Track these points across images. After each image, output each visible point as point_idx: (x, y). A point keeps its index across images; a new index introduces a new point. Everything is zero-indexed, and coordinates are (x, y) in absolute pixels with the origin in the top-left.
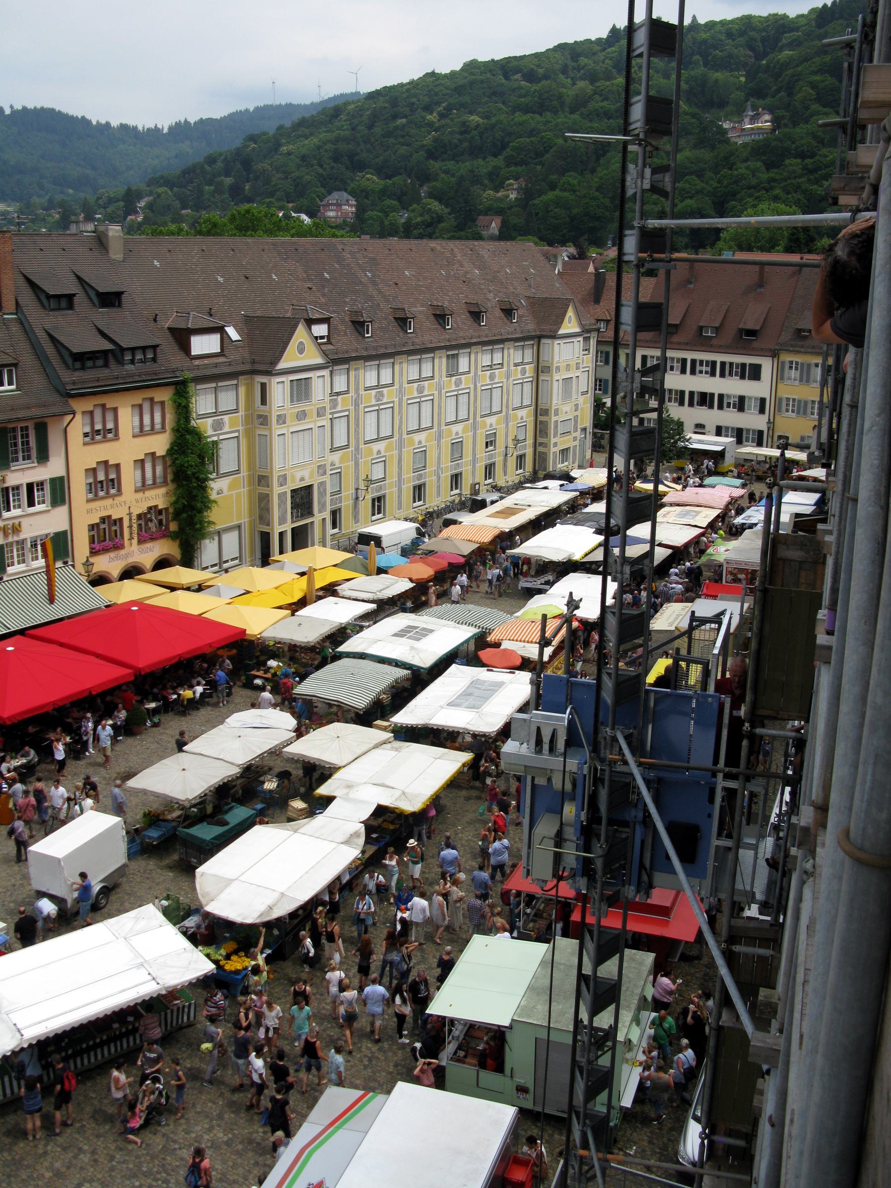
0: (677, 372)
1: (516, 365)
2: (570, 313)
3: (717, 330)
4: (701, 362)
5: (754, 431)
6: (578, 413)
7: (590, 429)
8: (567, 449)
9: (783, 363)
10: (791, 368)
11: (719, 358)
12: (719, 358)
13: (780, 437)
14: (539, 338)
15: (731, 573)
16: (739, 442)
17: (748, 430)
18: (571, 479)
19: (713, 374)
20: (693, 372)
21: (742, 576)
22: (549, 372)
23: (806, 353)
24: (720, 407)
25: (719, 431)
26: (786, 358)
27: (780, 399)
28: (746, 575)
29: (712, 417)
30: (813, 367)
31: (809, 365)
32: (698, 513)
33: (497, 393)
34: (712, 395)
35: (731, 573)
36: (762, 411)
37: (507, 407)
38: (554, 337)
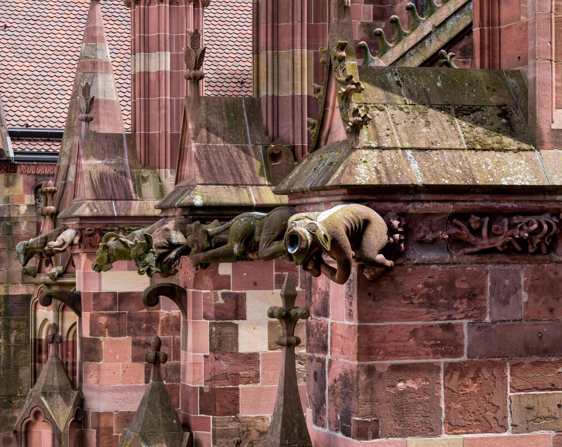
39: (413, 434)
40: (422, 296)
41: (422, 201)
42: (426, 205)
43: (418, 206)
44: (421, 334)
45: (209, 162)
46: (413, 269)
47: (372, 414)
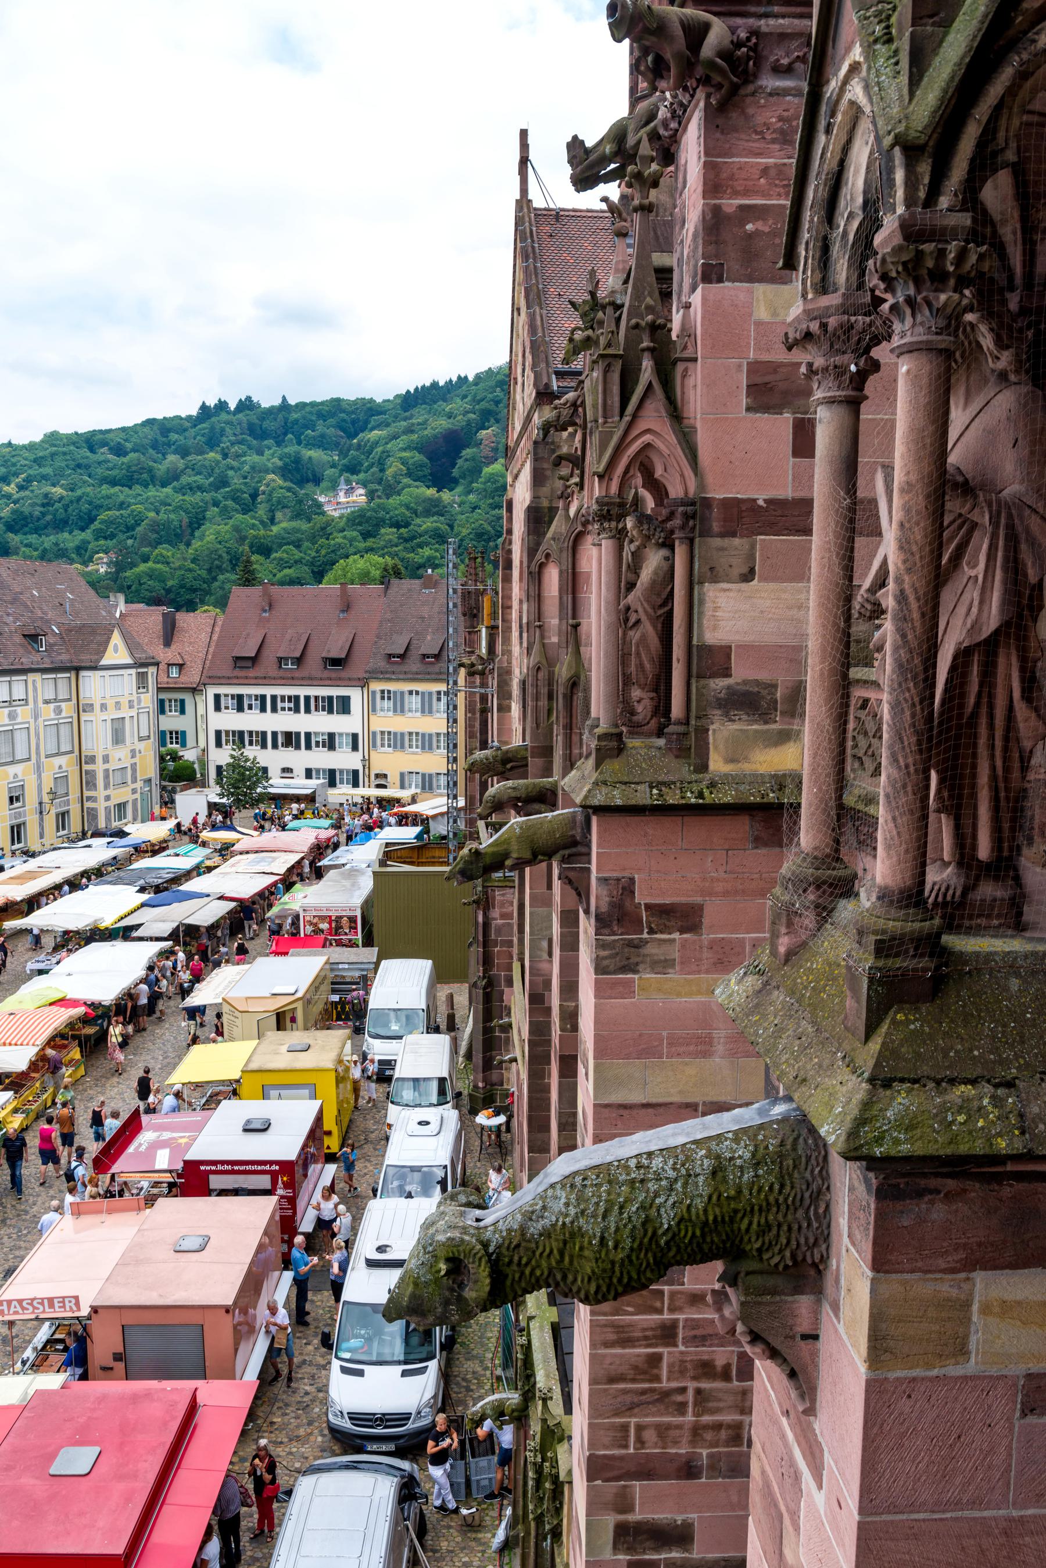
0: (256, 711)
1: (47, 702)
2: (116, 638)
3: (299, 661)
4: (283, 698)
5: (348, 771)
6: (136, 760)
7: (156, 781)
8: (125, 804)
9: (374, 692)
10: (383, 698)
11: (302, 692)
12: (302, 692)
13: (377, 776)
14: (78, 669)
15: (311, 923)
16: (332, 784)
17: (341, 771)
18: (121, 834)
19: (297, 710)
20: (274, 709)
21: (324, 926)
22: (92, 710)
23: (398, 680)
24: (308, 747)
25: (309, 774)
26: (376, 686)
27: (374, 733)
28: (330, 923)
29: (299, 759)
30: (407, 696)
31: (402, 693)
32: (274, 859)
33: (20, 738)
34: (298, 734)
35: (311, 923)
36: (355, 748)
37: (38, 753)
38: (95, 668)
39: (760, 280)
40: (775, 131)
41: (776, 16)
42: (781, 21)
43: (772, 22)
44: (773, 172)
45: (655, 233)
46: (767, 101)
47: (717, 256)
